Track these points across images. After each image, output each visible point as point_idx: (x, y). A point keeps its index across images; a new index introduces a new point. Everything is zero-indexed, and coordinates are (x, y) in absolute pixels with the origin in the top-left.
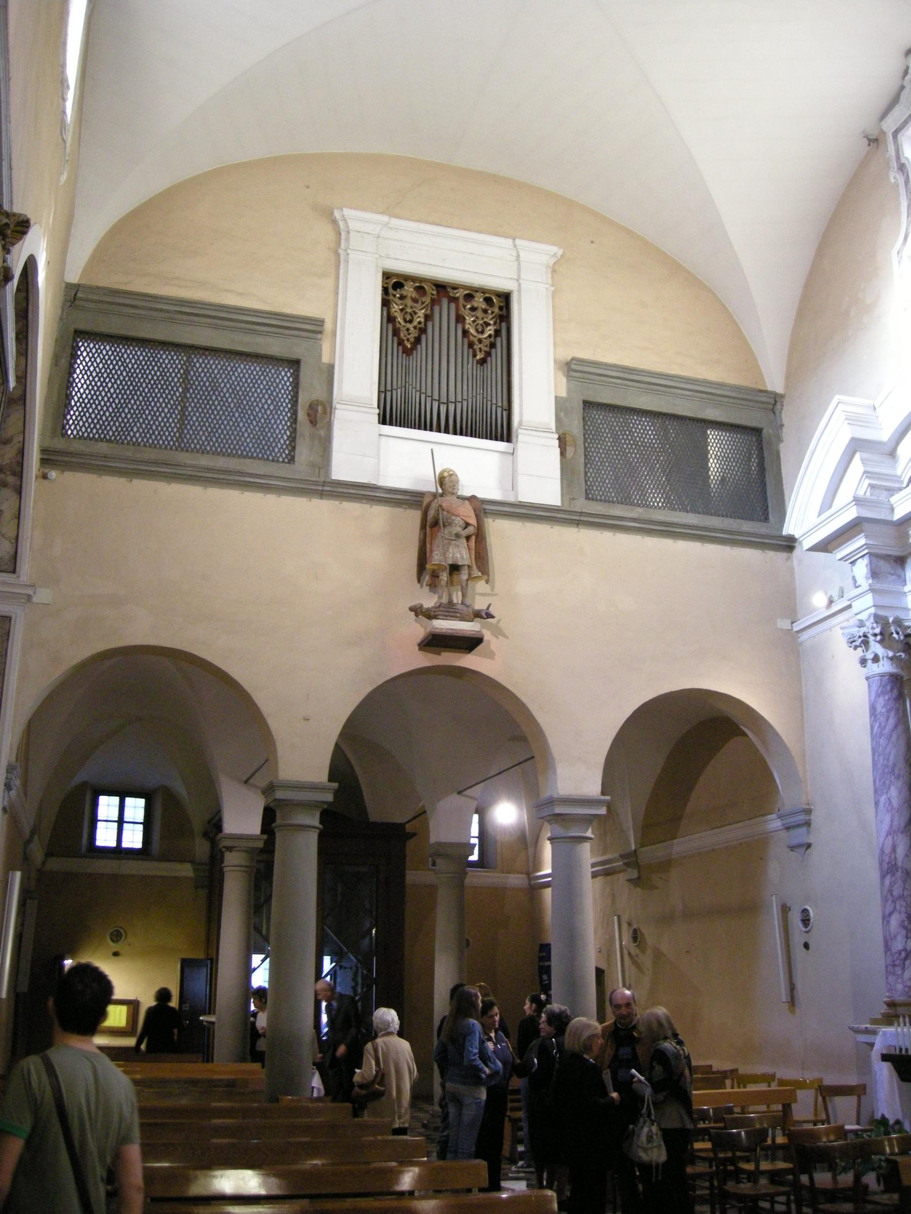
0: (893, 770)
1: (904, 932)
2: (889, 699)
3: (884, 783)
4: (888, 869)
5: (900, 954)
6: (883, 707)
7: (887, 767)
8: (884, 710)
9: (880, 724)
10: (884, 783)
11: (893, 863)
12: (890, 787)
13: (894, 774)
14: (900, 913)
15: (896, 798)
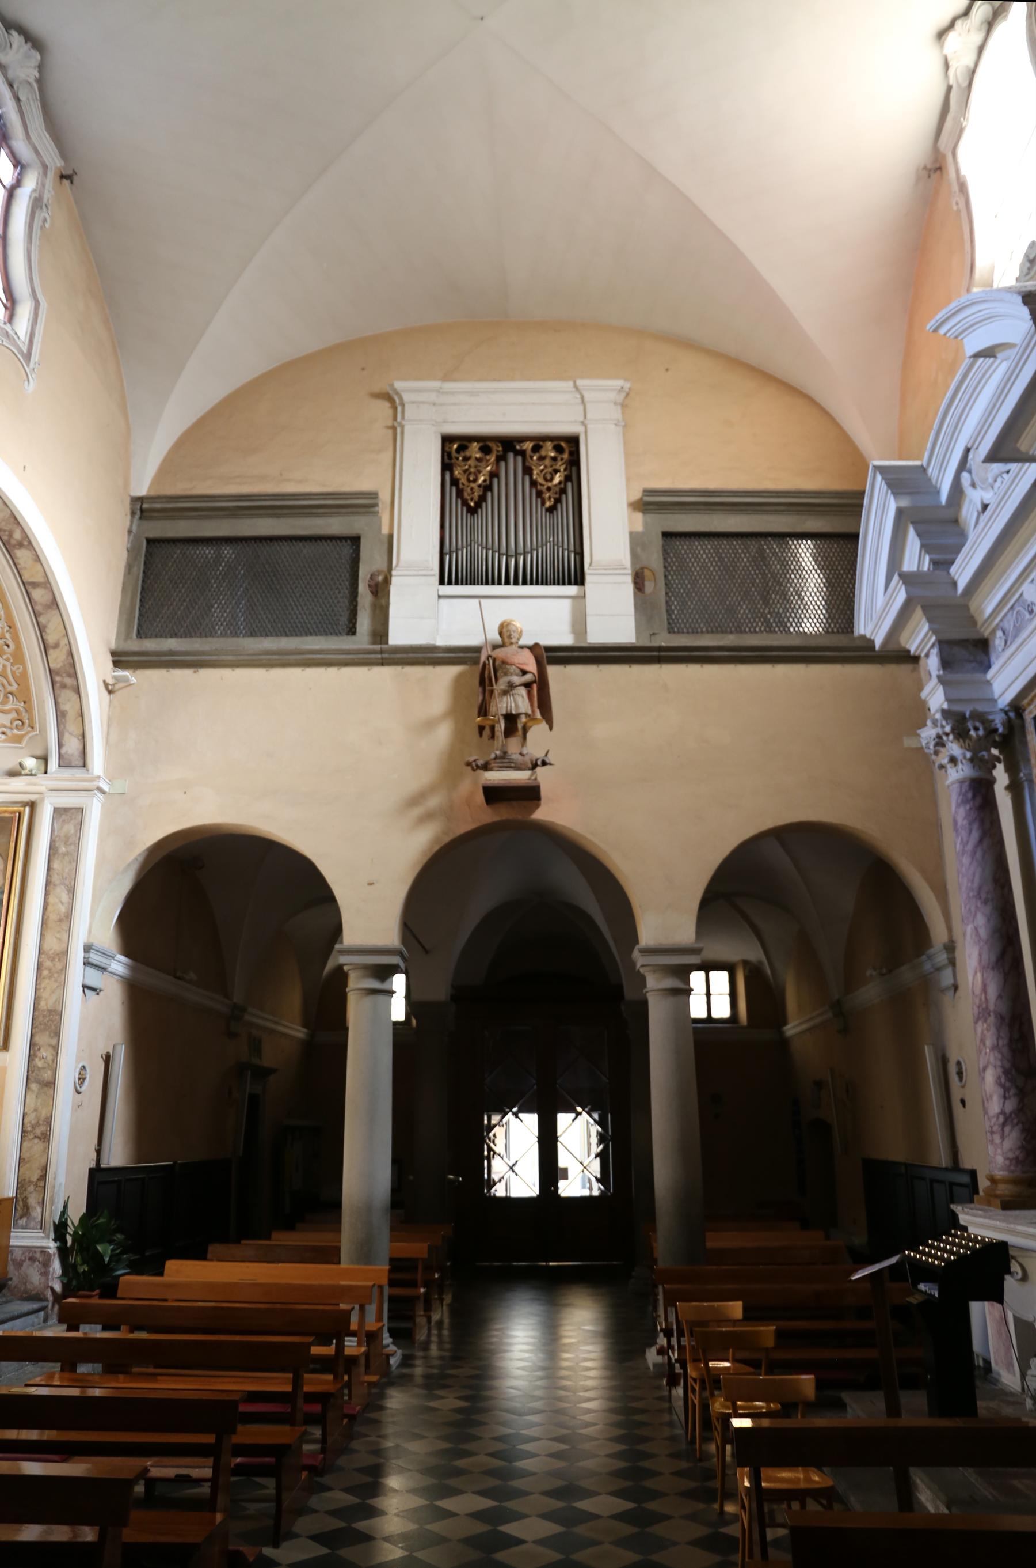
1: (1001, 1091)
2: (971, 809)
3: (970, 910)
4: (979, 1013)
5: (998, 1118)
6: (964, 819)
9: (962, 839)
10: (970, 910)
11: (984, 1006)
13: (980, 898)
14: (995, 1067)
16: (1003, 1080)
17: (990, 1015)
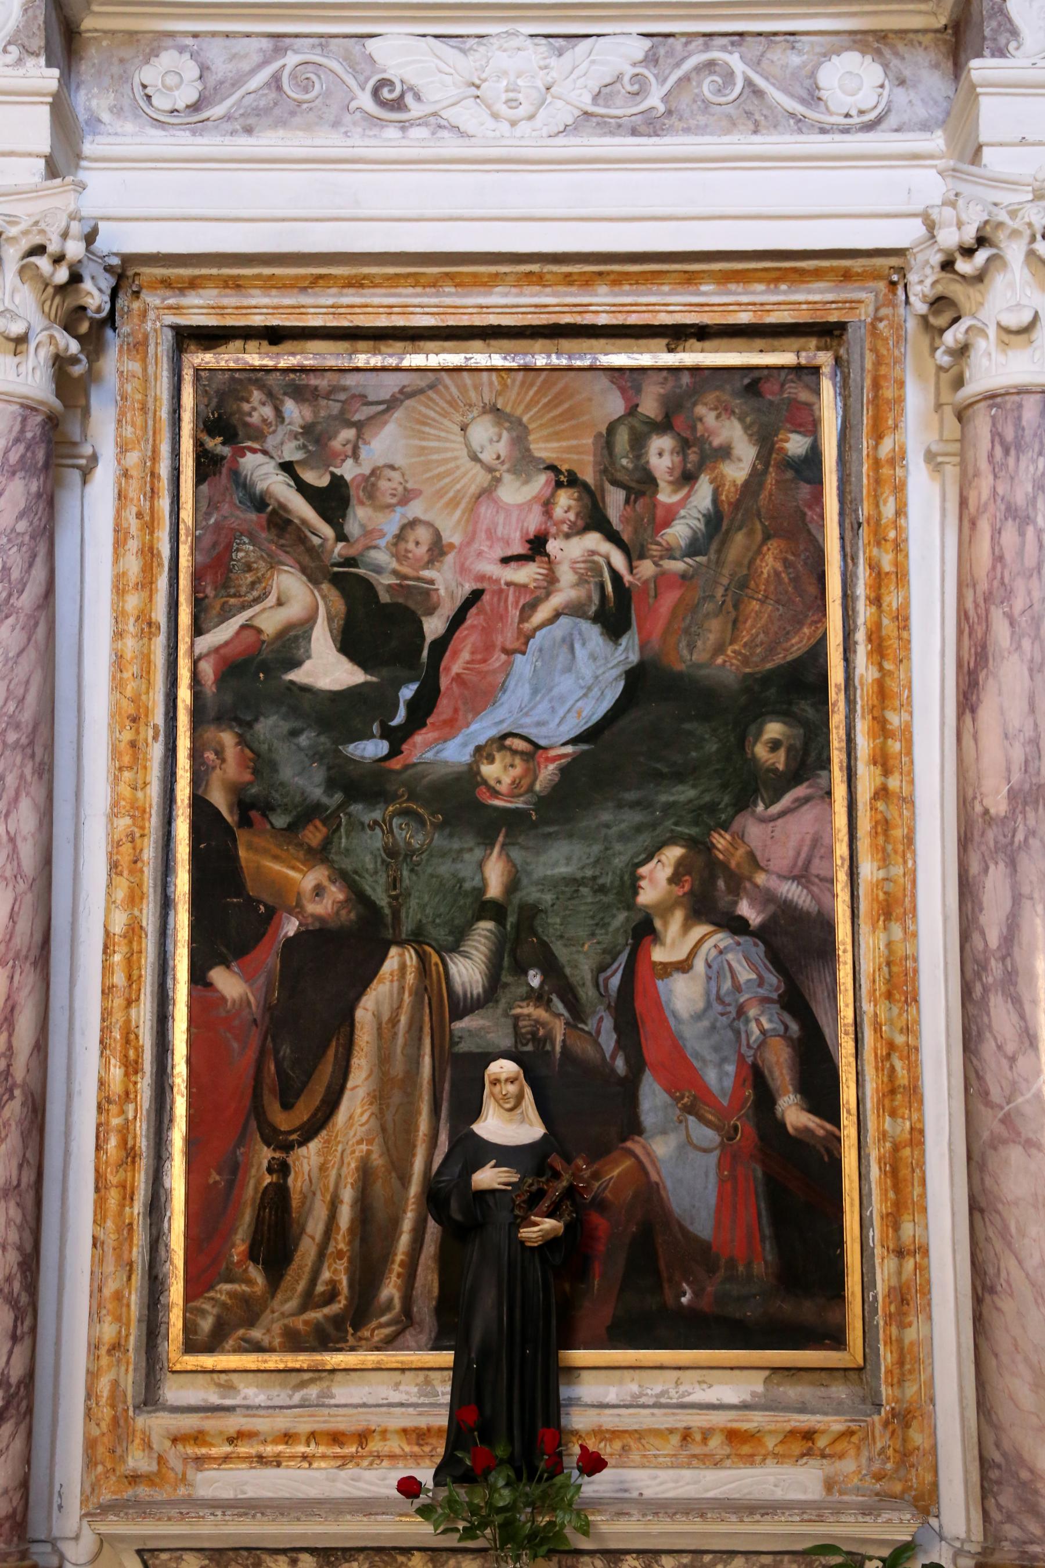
0: (31, 743)
2: (39, 495)
6: (21, 515)
7: (17, 726)
8: (22, 526)
12: (16, 799)
13: (33, 756)
15: (30, 842)
16: (17, 1286)
17: (12, 1097)
